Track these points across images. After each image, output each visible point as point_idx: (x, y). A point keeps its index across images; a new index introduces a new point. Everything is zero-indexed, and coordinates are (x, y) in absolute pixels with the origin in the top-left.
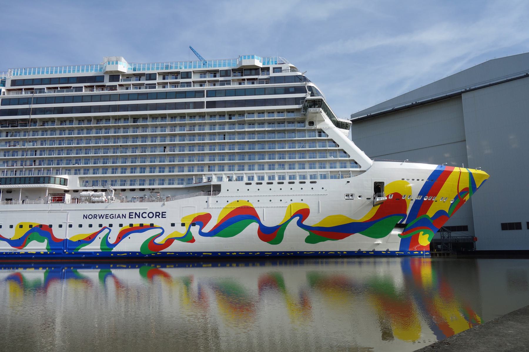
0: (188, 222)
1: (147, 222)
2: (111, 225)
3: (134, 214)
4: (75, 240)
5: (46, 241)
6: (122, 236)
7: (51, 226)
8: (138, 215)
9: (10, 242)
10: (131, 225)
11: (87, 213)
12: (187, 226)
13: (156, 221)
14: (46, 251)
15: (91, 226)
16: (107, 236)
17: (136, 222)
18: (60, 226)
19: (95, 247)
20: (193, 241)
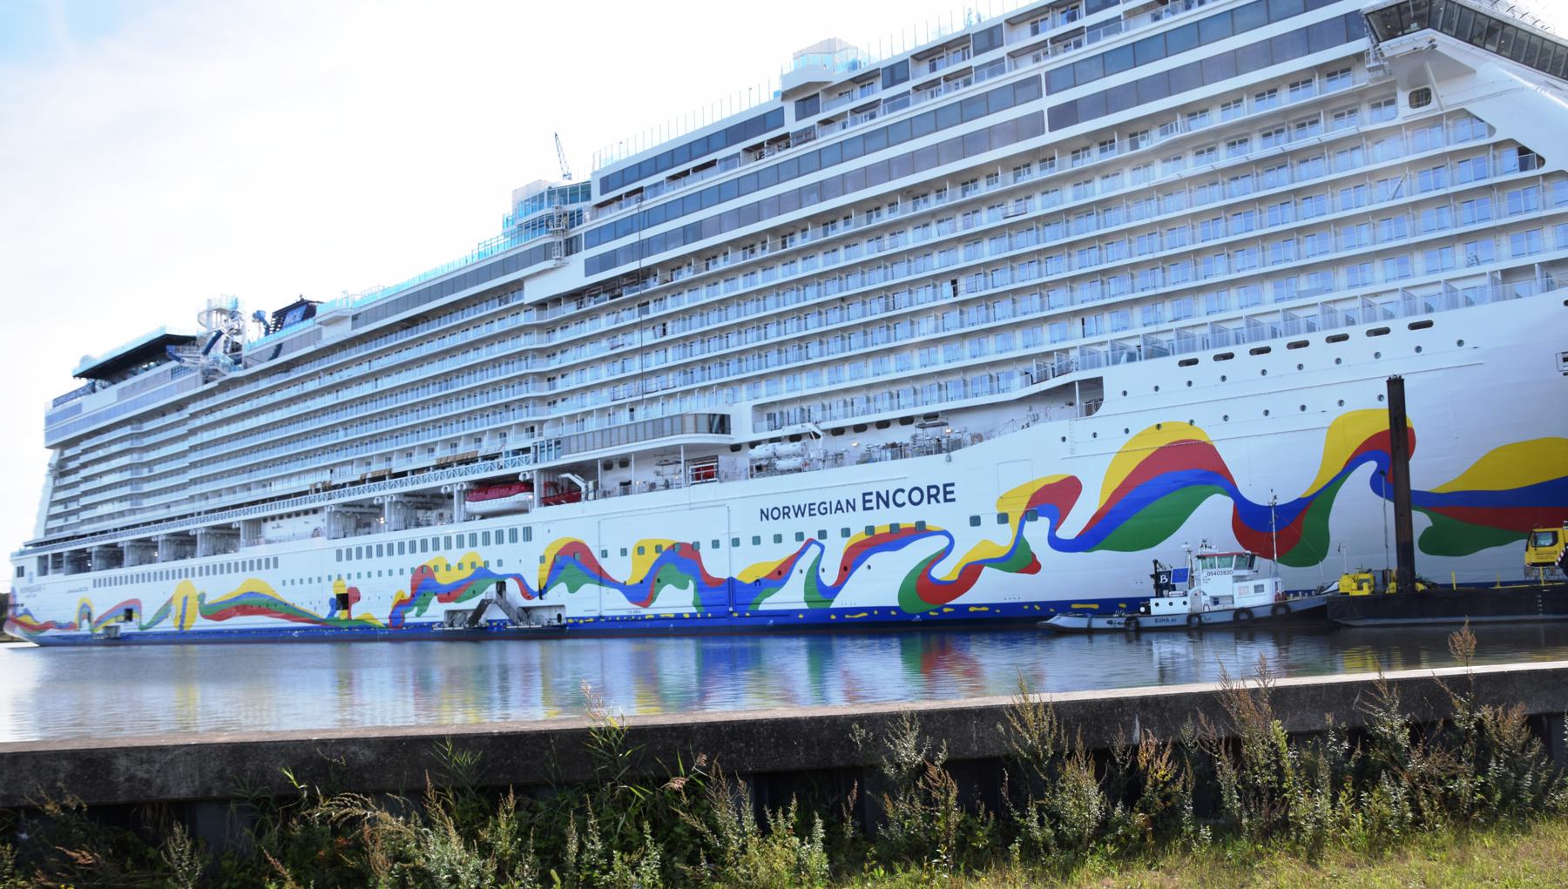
0: (1016, 510)
1: (907, 517)
2: (823, 534)
3: (874, 497)
4: (749, 580)
6: (853, 560)
8: (884, 500)
9: (622, 587)
10: (870, 529)
11: (768, 505)
12: (1014, 519)
13: (932, 515)
14: (694, 610)
17: (882, 519)
19: (790, 597)
20: (1033, 567)
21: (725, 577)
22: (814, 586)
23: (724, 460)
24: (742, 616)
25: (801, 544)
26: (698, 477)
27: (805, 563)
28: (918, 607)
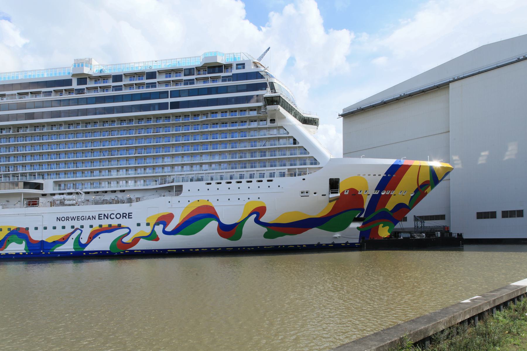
1: (115, 222)
2: (82, 227)
4: (50, 241)
5: (24, 242)
6: (93, 236)
7: (27, 229)
8: (106, 217)
10: (101, 226)
11: (60, 216)
13: (124, 222)
14: (25, 252)
15: (64, 227)
16: (79, 237)
17: (105, 223)
18: (36, 228)
19: (69, 247)
20: (157, 239)
21: (40, 240)
22: (78, 244)
23: (42, 200)
24: (46, 253)
25: (73, 230)
26: (29, 205)
27: (74, 236)
28: (116, 251)
